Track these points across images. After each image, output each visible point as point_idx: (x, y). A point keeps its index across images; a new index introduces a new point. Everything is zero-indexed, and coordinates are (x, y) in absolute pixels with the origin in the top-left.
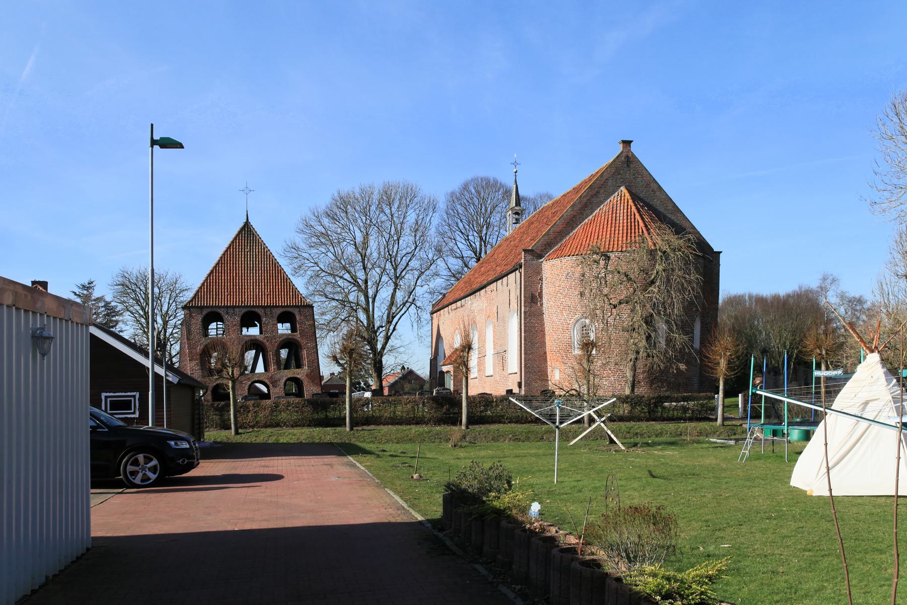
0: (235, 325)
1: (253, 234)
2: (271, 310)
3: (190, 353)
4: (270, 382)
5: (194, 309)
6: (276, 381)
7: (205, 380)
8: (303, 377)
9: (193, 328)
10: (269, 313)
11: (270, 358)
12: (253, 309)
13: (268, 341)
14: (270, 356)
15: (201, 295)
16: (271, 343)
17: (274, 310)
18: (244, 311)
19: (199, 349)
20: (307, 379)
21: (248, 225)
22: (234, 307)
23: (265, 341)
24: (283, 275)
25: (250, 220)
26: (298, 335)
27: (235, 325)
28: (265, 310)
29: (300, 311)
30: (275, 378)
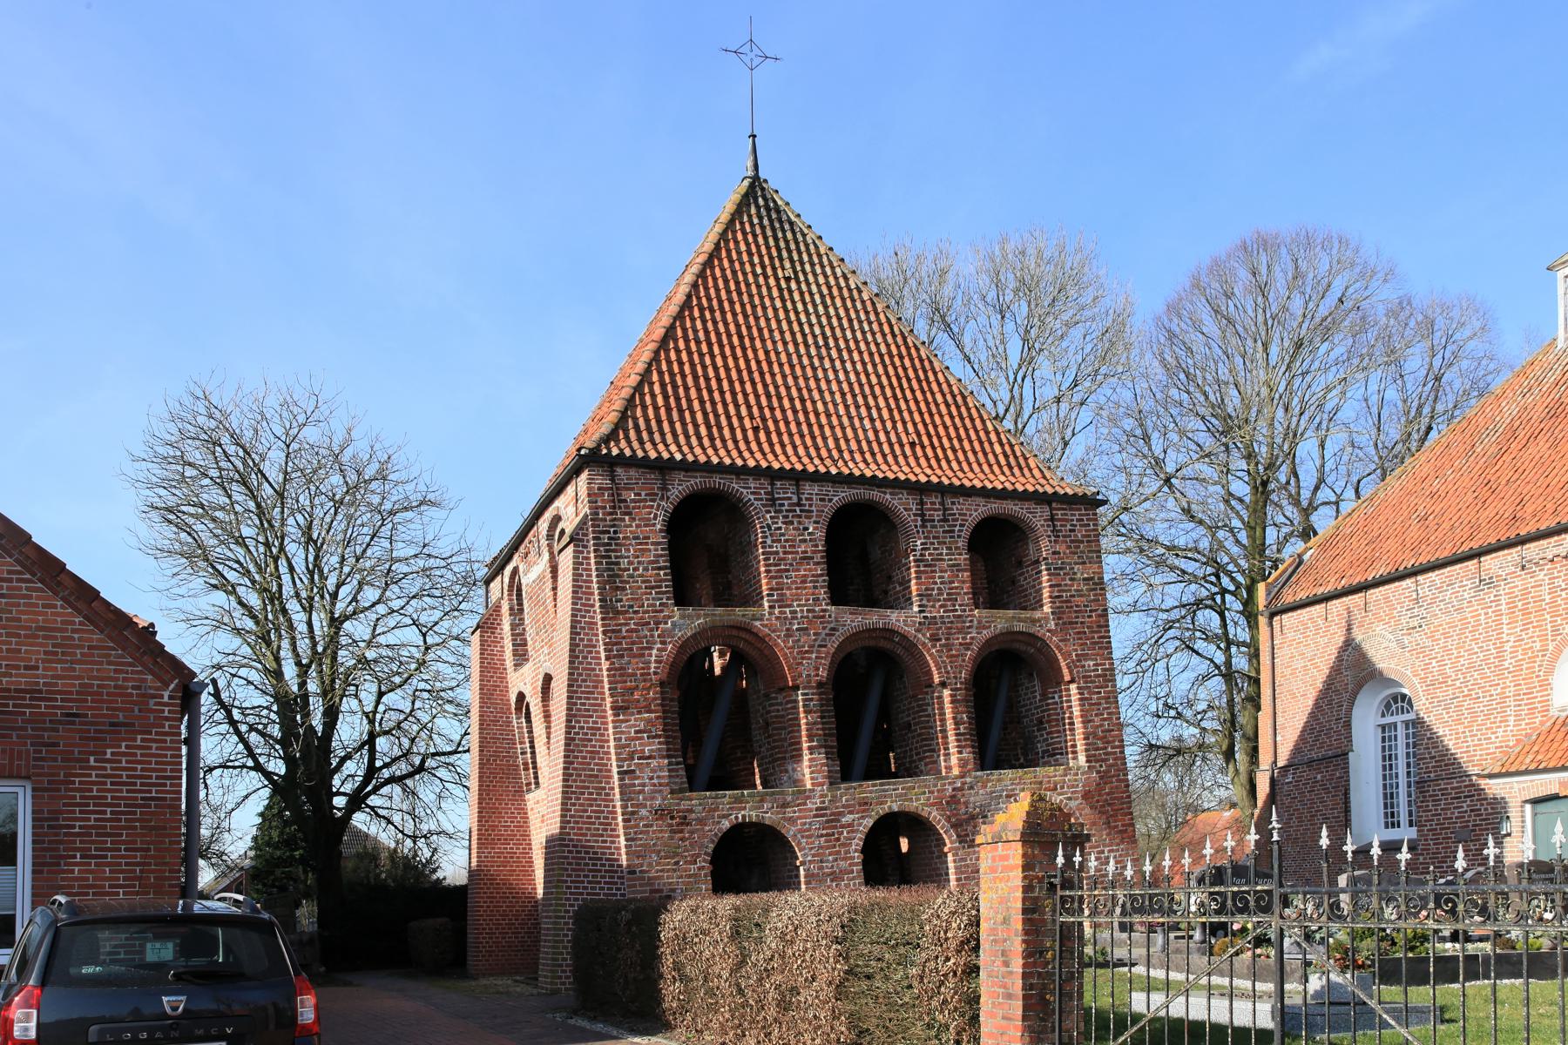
0: (806, 559)
1: (791, 224)
2: (942, 503)
3: (617, 674)
4: (948, 819)
5: (633, 472)
6: (973, 817)
7: (685, 805)
8: (1073, 804)
9: (627, 556)
10: (937, 516)
11: (942, 714)
12: (875, 495)
13: (935, 639)
14: (942, 708)
15: (647, 421)
16: (949, 647)
17: (959, 506)
18: (842, 495)
19: (658, 657)
20: (1087, 810)
21: (756, 189)
22: (798, 478)
23: (923, 638)
24: (947, 381)
25: (762, 175)
26: (1046, 619)
27: (806, 559)
28: (922, 503)
29: (1052, 519)
30: (966, 804)
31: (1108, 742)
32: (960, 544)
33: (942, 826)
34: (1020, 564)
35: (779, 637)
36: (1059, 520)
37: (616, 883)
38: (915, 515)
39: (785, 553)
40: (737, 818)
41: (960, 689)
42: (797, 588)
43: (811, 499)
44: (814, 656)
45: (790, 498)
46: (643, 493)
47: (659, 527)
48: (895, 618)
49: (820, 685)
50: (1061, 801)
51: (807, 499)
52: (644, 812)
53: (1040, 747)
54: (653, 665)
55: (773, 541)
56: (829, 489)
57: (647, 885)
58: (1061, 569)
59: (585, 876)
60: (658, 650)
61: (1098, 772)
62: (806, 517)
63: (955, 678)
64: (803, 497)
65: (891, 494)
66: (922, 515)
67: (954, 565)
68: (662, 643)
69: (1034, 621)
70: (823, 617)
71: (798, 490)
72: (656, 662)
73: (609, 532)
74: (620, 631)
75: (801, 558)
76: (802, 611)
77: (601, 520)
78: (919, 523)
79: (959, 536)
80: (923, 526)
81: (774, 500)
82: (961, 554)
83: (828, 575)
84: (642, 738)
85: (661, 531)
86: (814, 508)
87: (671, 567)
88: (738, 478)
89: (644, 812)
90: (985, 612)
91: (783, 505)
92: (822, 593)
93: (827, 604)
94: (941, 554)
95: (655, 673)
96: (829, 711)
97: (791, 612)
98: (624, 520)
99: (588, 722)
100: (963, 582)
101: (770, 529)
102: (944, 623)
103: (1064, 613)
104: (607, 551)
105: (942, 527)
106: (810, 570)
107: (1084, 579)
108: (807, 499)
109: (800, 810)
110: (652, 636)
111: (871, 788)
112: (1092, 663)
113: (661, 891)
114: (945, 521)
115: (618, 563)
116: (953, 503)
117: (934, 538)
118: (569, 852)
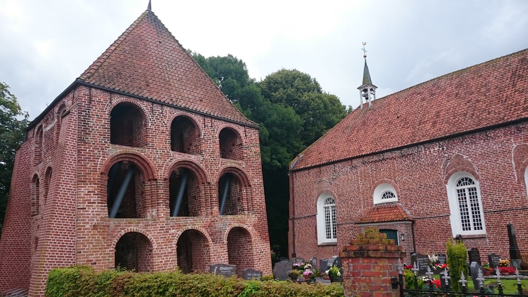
5: (99, 91)
9: (93, 122)
10: (210, 125)
12: (189, 114)
13: (206, 166)
17: (217, 123)
18: (177, 113)
31: (261, 207)
32: (216, 135)
33: (207, 235)
34: (234, 145)
35: (151, 160)
36: (247, 132)
37: (71, 257)
38: (202, 123)
39: (155, 129)
40: (128, 230)
41: (214, 185)
42: (159, 143)
43: (166, 112)
44: (163, 168)
45: (159, 111)
46: (102, 100)
47: (107, 113)
48: (193, 158)
49: (165, 179)
50: (246, 227)
51: (165, 112)
52: (88, 226)
53: (238, 208)
54: (98, 165)
55: (151, 125)
56: (173, 110)
57: (86, 258)
58: (247, 148)
59: (57, 254)
60: (102, 159)
61: (258, 217)
62: (164, 118)
63: (213, 181)
64: (164, 111)
65: (194, 115)
66: (204, 124)
67: (214, 142)
68: (103, 157)
69: (239, 164)
70: (168, 154)
71: (162, 108)
72: (100, 164)
73: (86, 112)
74: (86, 150)
75: (161, 132)
76: (160, 151)
77: (83, 106)
78: (203, 126)
79: (216, 133)
80: (205, 127)
81: (153, 110)
82: (216, 139)
83: (171, 139)
84: (91, 195)
85: (108, 114)
86: (167, 115)
87: (111, 128)
88: (140, 100)
89: (88, 226)
90: (224, 159)
91: (156, 112)
92: (168, 146)
93: (169, 150)
94: (210, 138)
95: (99, 169)
96: (167, 190)
97: (156, 151)
98: (93, 108)
99: (67, 186)
100: (217, 148)
101: (151, 120)
102: (210, 161)
103: (248, 162)
104: (84, 118)
105: (211, 129)
106: (164, 137)
107: (254, 152)
108: (165, 112)
109: (154, 228)
110: (100, 154)
111: (182, 220)
112: (256, 180)
113: (92, 261)
114: (212, 127)
115: (88, 124)
116: (215, 121)
117: (208, 132)
118: (51, 243)
